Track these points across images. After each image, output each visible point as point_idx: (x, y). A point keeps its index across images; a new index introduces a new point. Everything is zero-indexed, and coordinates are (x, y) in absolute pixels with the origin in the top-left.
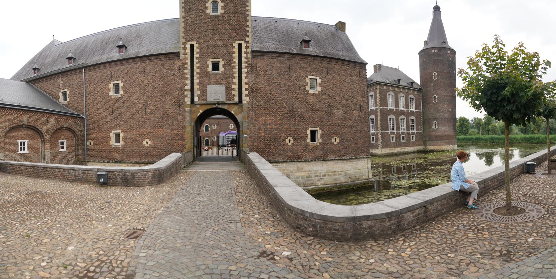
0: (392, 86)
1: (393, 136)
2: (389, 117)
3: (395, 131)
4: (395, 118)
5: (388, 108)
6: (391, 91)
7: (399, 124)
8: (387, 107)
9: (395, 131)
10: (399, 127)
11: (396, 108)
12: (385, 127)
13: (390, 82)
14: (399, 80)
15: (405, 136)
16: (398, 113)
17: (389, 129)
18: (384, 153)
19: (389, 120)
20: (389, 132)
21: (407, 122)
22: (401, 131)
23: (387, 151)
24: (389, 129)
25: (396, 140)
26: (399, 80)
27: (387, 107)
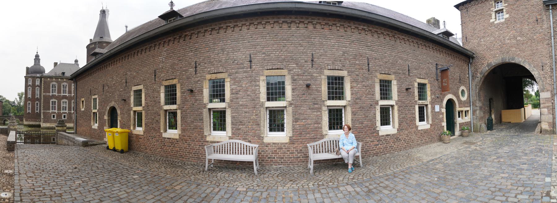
0: (55, 78)
1: (54, 114)
2: (51, 101)
3: (56, 111)
4: (57, 101)
5: (51, 94)
6: (54, 81)
7: (61, 106)
8: (50, 93)
9: (56, 111)
10: (61, 108)
11: (58, 93)
12: (47, 107)
13: (56, 75)
14: (63, 73)
15: (66, 115)
16: (59, 98)
17: (51, 109)
18: (45, 126)
19: (51, 103)
20: (51, 111)
21: (68, 104)
22: (62, 111)
23: (48, 125)
24: (51, 109)
25: (57, 117)
26: (63, 73)
27: (50, 93)
